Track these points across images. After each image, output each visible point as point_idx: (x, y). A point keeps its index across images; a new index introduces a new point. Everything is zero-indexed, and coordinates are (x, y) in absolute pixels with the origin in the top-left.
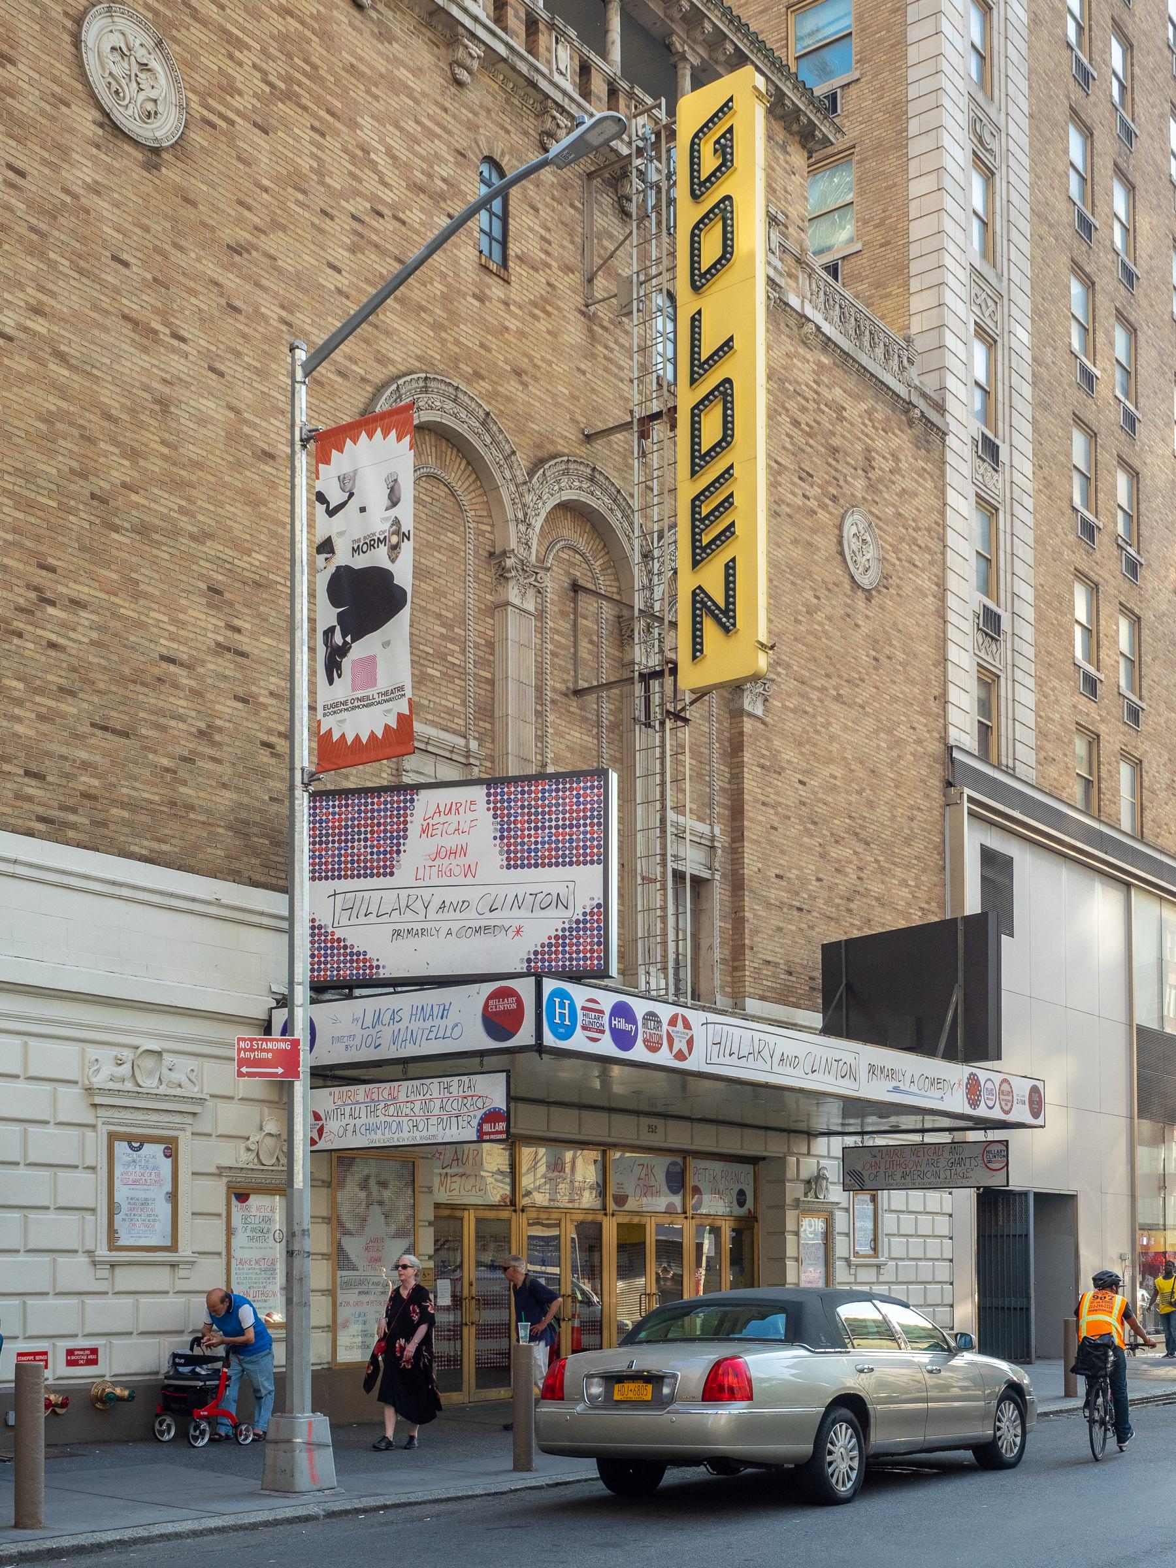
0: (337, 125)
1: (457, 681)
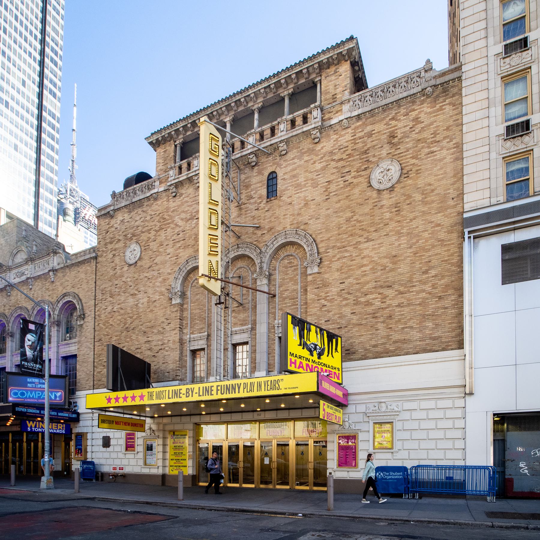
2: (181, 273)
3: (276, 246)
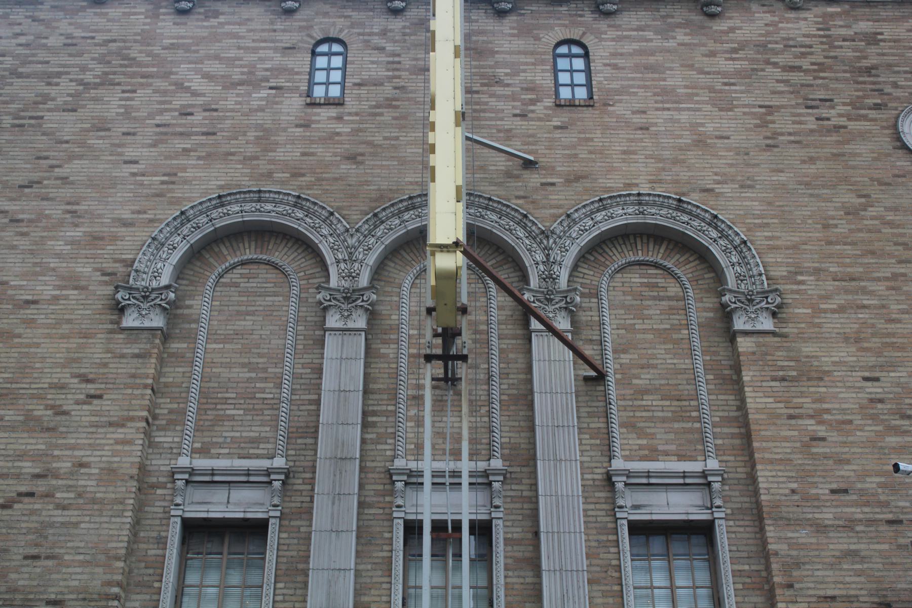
0: (150, 80)
1: (266, 412)
2: (185, 230)
3: (604, 227)
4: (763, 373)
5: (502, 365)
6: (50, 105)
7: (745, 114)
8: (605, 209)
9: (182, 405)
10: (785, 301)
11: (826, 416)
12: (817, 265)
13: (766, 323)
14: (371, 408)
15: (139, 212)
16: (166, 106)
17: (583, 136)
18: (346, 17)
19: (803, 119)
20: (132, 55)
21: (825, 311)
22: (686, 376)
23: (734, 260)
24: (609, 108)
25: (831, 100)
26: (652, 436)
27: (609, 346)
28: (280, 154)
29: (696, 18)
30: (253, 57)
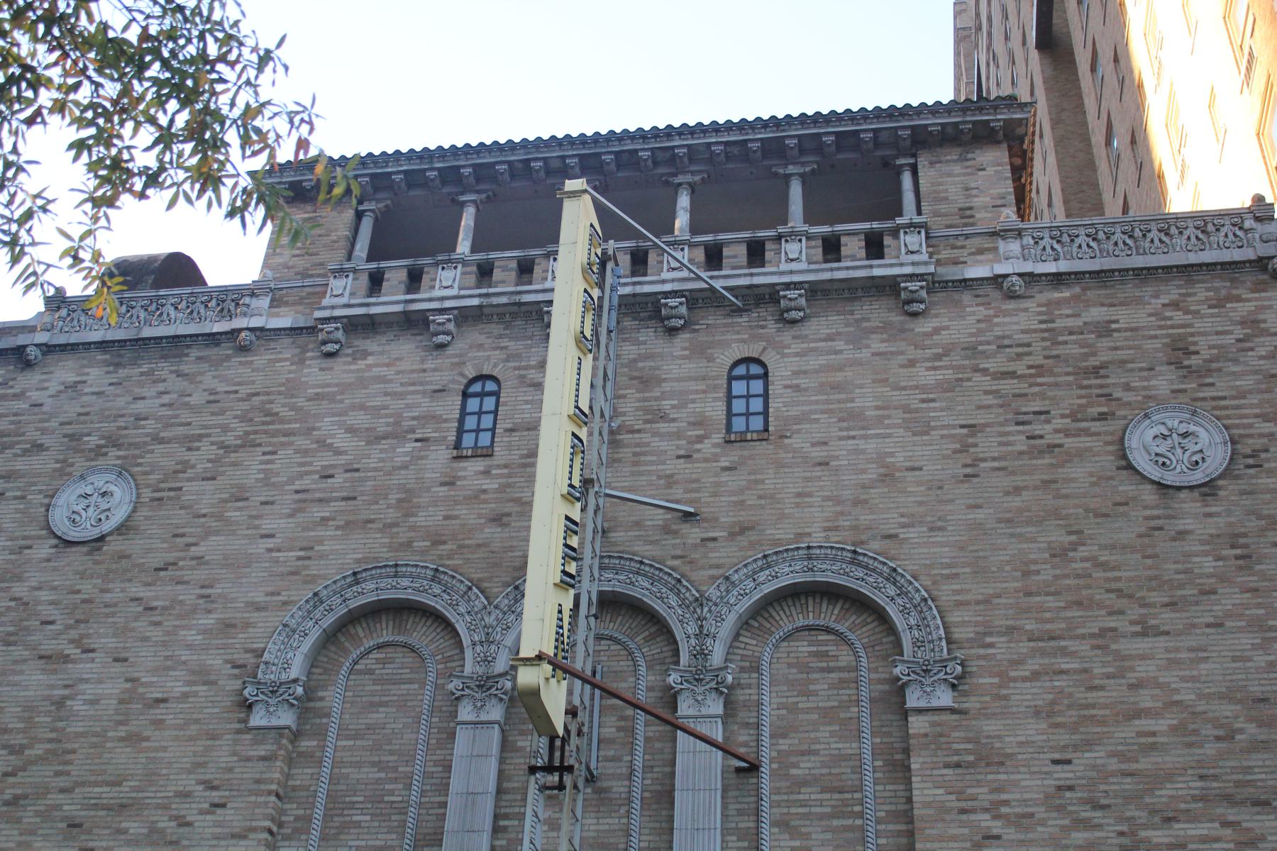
0: (292, 439)
1: (394, 818)
3: (768, 589)
4: (935, 759)
5: (647, 757)
6: (190, 473)
7: (943, 437)
8: (769, 567)
9: (308, 812)
10: (969, 669)
11: (1004, 810)
12: (1010, 623)
13: (944, 698)
14: (503, 811)
15: (272, 594)
16: (307, 469)
17: (753, 477)
18: (502, 348)
19: (1011, 438)
20: (275, 410)
21: (1015, 680)
22: (852, 763)
23: (913, 622)
24: (787, 441)
25: (1047, 412)
26: (807, 836)
27: (766, 731)
28: (421, 519)
29: (896, 318)
30: (400, 404)
